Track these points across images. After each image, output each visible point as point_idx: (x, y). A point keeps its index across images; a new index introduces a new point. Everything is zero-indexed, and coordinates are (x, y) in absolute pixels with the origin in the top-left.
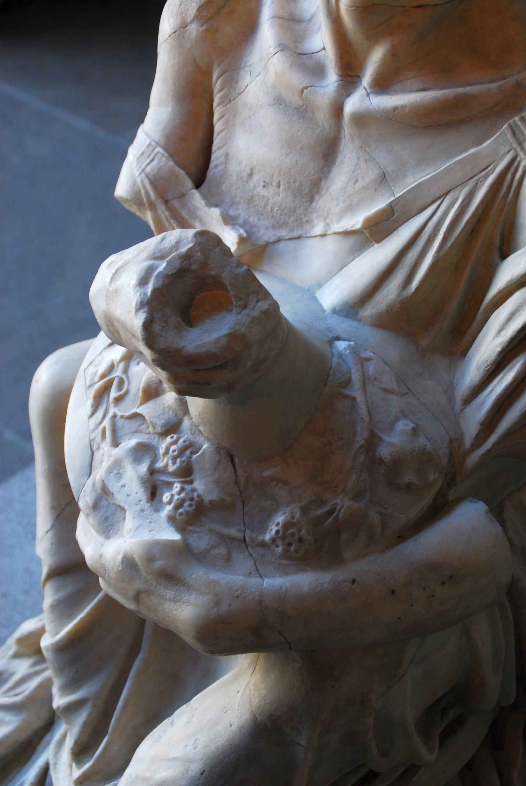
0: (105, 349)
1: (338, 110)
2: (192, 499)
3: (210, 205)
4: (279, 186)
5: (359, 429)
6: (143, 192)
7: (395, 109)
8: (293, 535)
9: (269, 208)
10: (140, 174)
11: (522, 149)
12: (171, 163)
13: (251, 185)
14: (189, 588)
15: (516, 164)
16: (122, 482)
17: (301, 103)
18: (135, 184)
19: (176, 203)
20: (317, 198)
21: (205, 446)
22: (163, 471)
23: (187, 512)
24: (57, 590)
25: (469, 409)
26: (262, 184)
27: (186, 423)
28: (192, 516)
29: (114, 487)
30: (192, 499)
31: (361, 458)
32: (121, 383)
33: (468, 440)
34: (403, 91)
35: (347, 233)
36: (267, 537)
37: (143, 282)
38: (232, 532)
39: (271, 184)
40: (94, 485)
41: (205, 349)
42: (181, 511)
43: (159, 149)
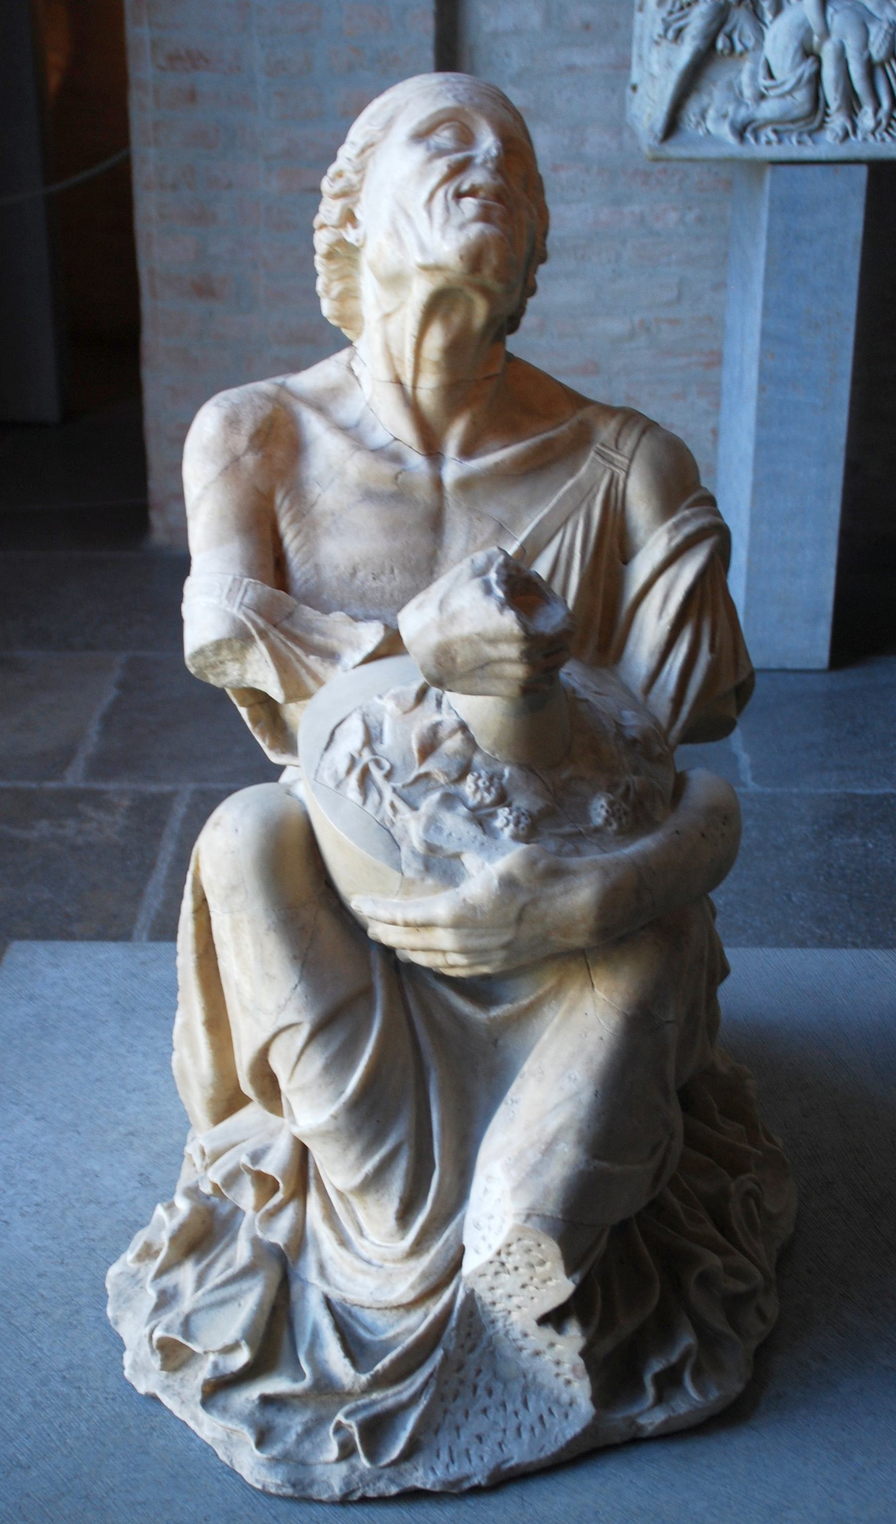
0: (322, 756)
1: (438, 483)
3: (327, 611)
4: (392, 571)
5: (604, 722)
6: (249, 625)
8: (618, 810)
9: (387, 596)
10: (239, 607)
11: (616, 466)
12: (268, 588)
13: (357, 582)
14: (573, 873)
16: (446, 833)
17: (394, 488)
18: (234, 620)
19: (286, 624)
20: (436, 569)
21: (507, 772)
22: (480, 806)
23: (527, 825)
24: (326, 1045)
25: (652, 697)
26: (370, 577)
27: (477, 759)
28: (530, 830)
29: (438, 840)
30: (523, 814)
32: (378, 764)
33: (664, 721)
34: (487, 452)
36: (598, 821)
38: (567, 829)
39: (383, 573)
40: (414, 852)
43: (246, 580)
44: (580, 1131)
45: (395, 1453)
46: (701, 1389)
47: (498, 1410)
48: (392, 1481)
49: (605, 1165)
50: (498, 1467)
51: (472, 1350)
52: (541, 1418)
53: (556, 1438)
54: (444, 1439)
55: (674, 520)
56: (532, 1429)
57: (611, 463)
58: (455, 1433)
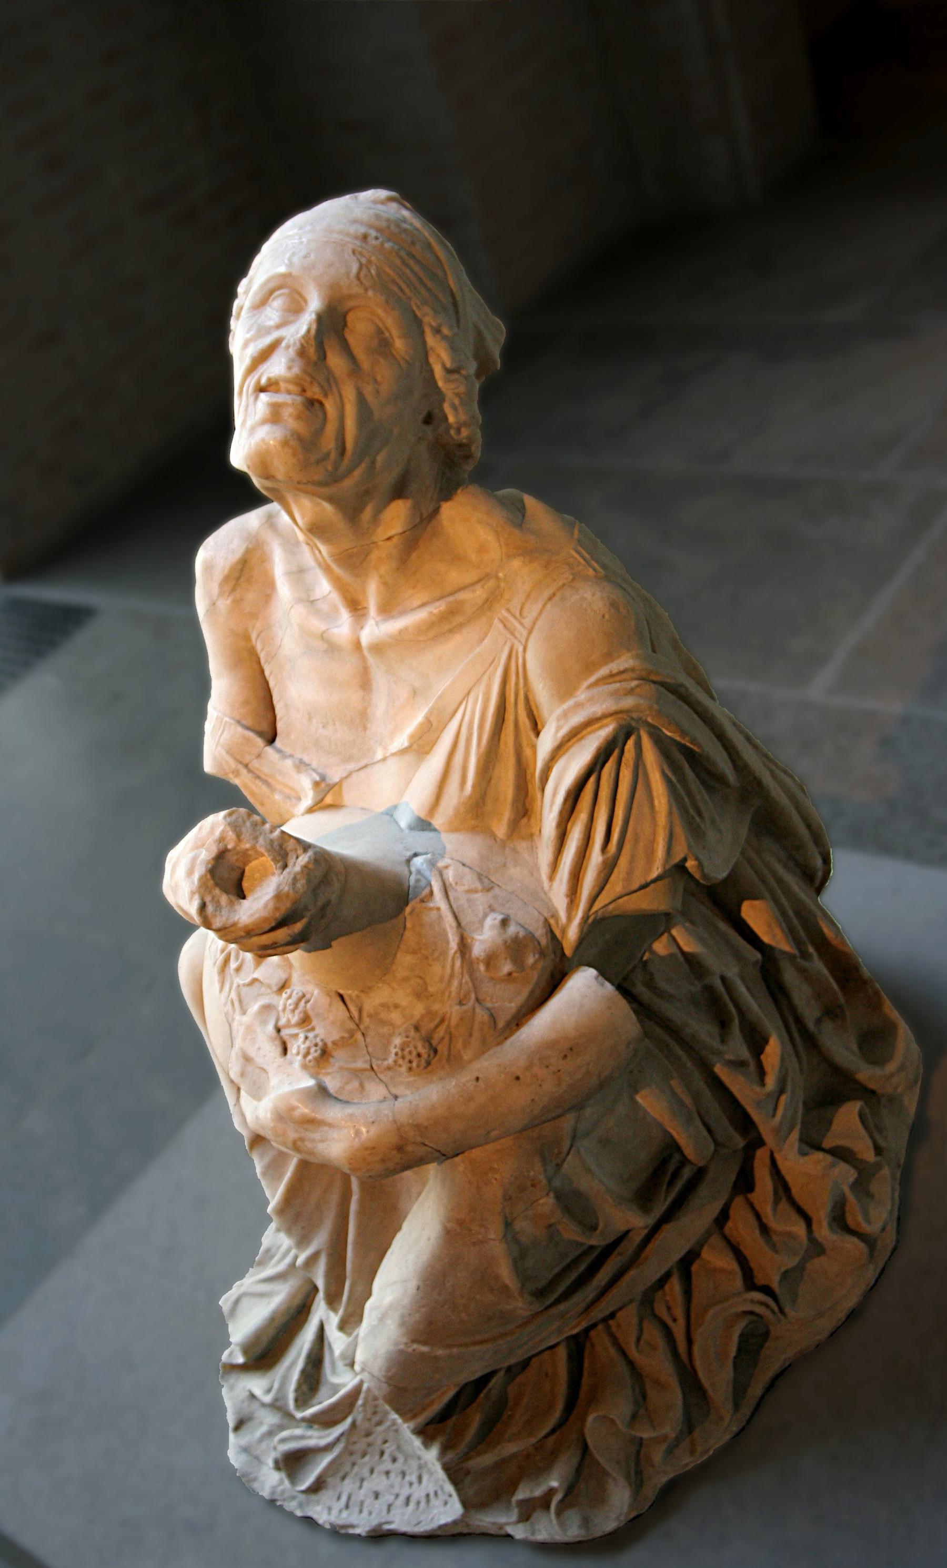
1: (358, 645)
2: (316, 1045)
7: (401, 632)
8: (410, 1053)
11: (516, 638)
15: (514, 652)
16: (257, 1046)
20: (369, 725)
26: (321, 726)
31: (458, 963)
35: (403, 752)
36: (390, 1061)
37: (190, 873)
41: (257, 916)
42: (310, 1057)
43: (227, 719)
44: (402, 1316)
45: (304, 1487)
46: (562, 1525)
47: (397, 1476)
48: (301, 1505)
49: (425, 1349)
50: (380, 1525)
51: (379, 1423)
52: (428, 1495)
53: (432, 1519)
54: (348, 1486)
55: (565, 706)
56: (418, 1503)
57: (512, 634)
58: (358, 1484)
